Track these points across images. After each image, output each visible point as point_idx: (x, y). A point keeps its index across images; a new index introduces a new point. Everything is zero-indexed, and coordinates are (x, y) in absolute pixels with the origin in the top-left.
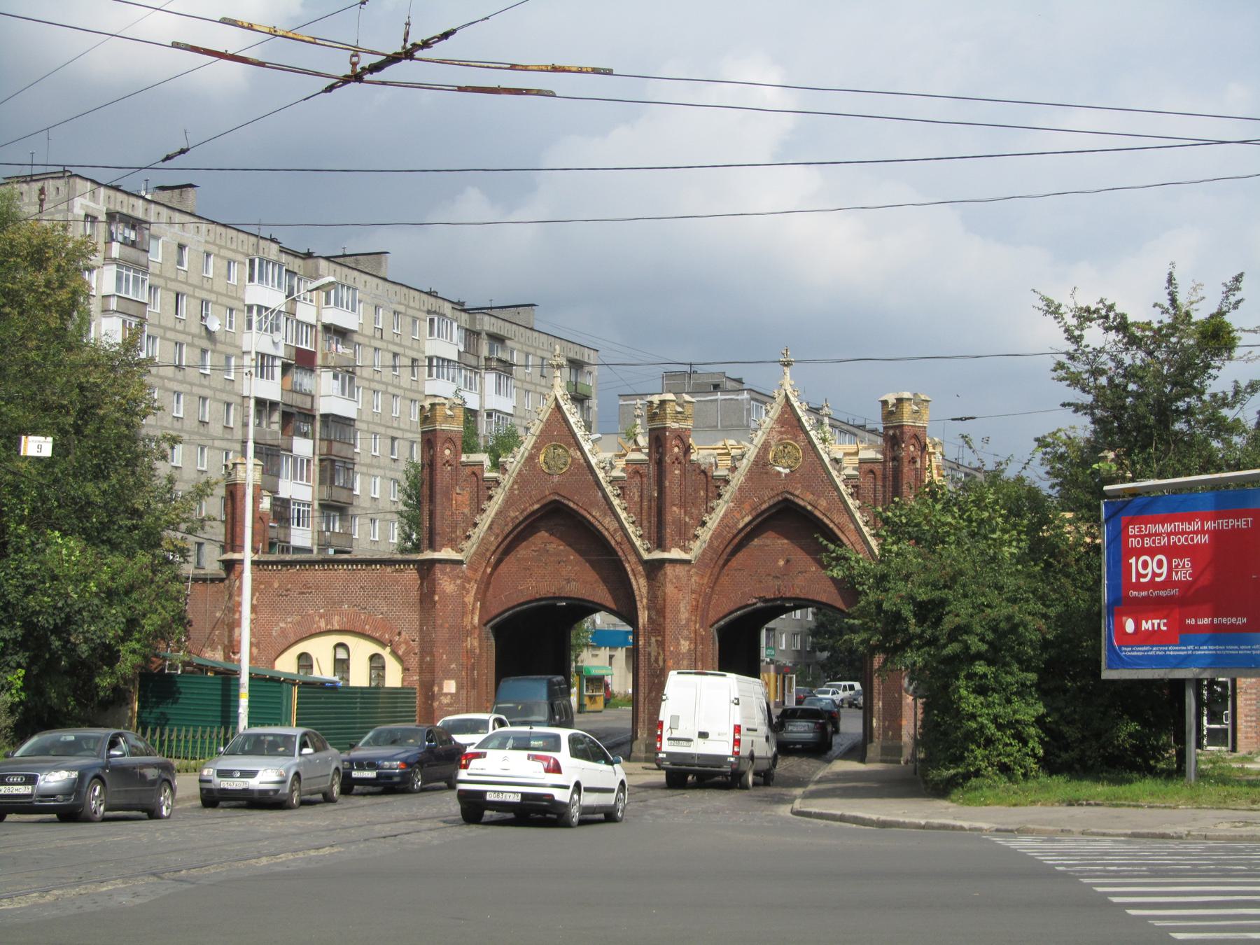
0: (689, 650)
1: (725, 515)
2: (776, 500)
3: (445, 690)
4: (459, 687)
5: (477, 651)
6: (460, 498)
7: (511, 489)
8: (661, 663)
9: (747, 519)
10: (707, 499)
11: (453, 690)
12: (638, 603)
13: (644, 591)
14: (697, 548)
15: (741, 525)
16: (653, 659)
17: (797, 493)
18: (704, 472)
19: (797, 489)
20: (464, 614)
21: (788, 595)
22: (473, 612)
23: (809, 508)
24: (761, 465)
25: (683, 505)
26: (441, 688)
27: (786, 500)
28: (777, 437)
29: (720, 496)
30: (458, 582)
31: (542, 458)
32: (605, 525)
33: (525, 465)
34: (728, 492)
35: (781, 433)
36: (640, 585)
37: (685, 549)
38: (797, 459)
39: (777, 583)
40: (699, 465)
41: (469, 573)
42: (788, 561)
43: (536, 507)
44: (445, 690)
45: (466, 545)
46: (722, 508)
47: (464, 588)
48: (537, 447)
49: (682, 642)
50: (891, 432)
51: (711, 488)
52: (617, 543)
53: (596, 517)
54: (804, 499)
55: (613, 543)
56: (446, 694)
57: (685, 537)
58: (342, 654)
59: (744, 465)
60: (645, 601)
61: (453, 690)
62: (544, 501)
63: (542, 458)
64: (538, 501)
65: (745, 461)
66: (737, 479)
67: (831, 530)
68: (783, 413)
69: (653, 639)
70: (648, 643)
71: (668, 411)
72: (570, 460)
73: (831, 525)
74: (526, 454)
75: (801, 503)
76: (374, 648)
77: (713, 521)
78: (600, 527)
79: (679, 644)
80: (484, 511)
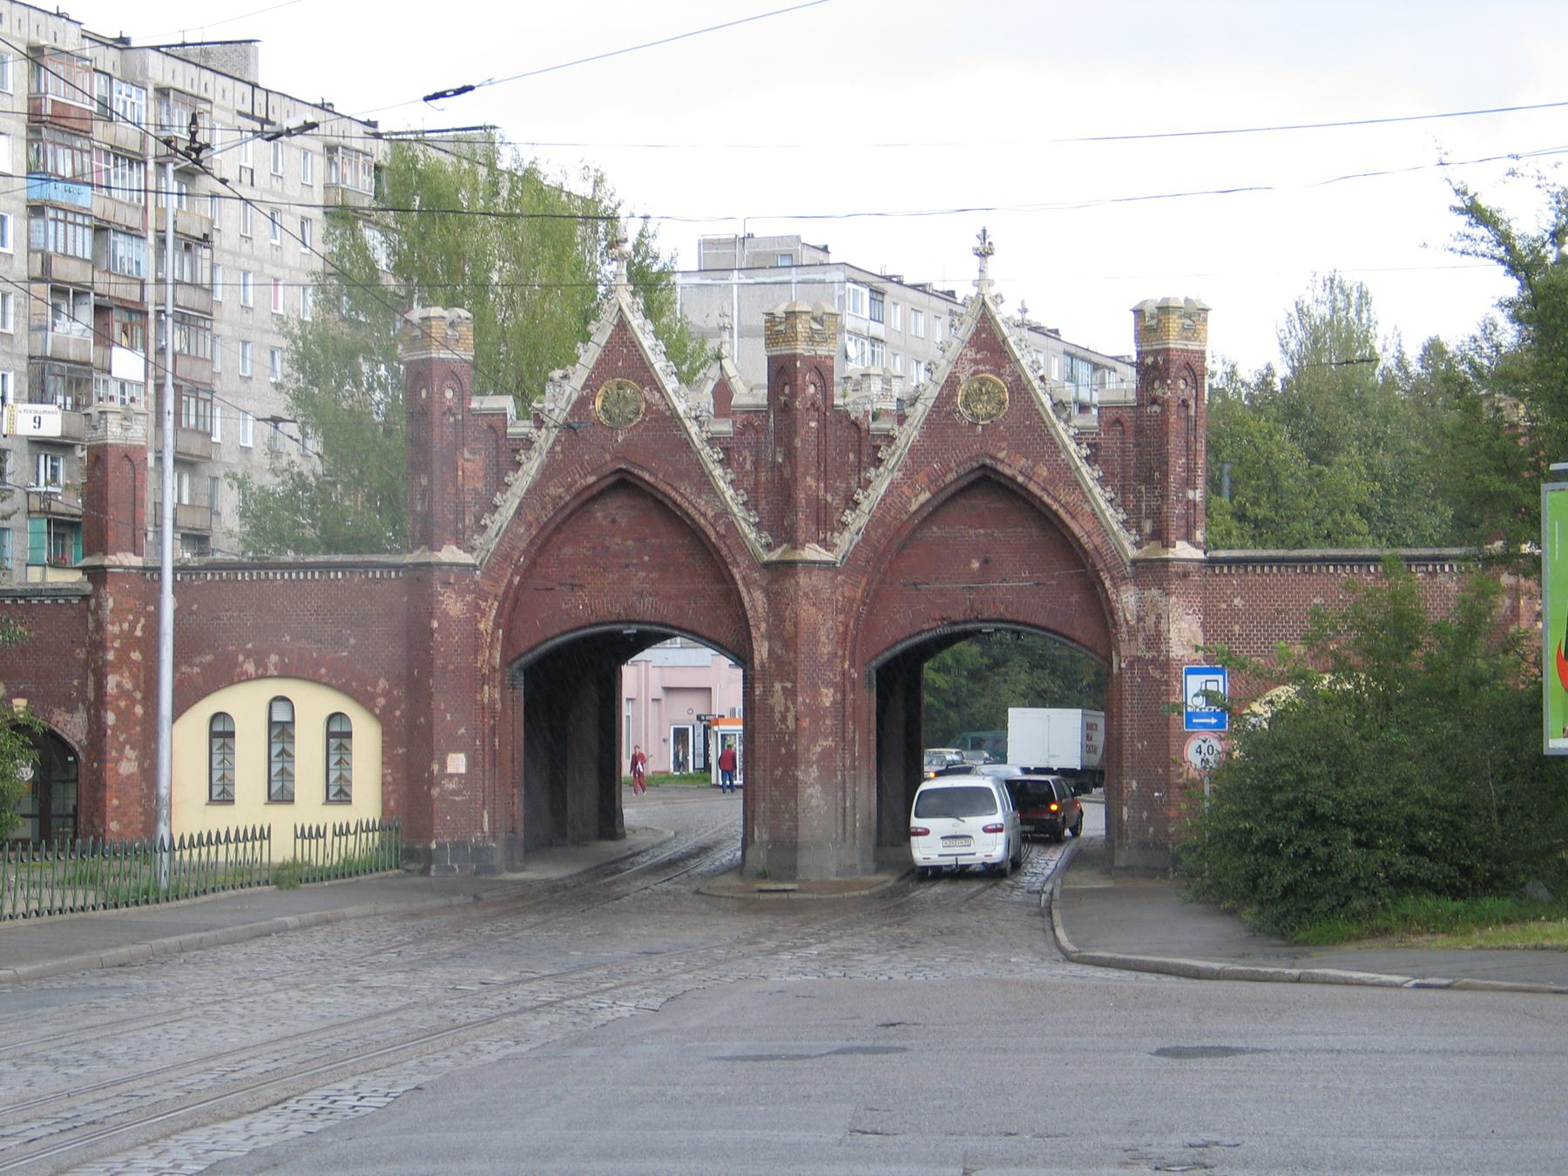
0: (834, 702)
1: (889, 492)
2: (968, 467)
3: (450, 770)
4: (471, 764)
5: (498, 706)
6: (468, 465)
7: (551, 451)
8: (791, 723)
9: (924, 497)
10: (860, 468)
11: (463, 770)
12: (753, 631)
14: (845, 542)
15: (914, 507)
16: (777, 716)
17: (1002, 455)
18: (855, 424)
19: (1001, 449)
20: (477, 649)
21: (986, 615)
22: (491, 647)
23: (1020, 479)
25: (823, 476)
26: (444, 765)
27: (984, 466)
28: (969, 369)
29: (878, 462)
30: (469, 598)
31: (599, 402)
32: (700, 508)
33: (572, 414)
34: (894, 458)
35: (976, 362)
36: (755, 601)
37: (828, 545)
40: (847, 414)
41: (487, 586)
42: (986, 561)
43: (591, 479)
44: (450, 770)
45: (478, 540)
46: (881, 482)
47: (477, 607)
48: (591, 385)
50: (1149, 360)
51: (866, 450)
52: (720, 536)
53: (684, 495)
54: (1013, 466)
55: (713, 537)
56: (452, 776)
57: (825, 523)
58: (280, 715)
59: (918, 413)
60: (763, 626)
61: (463, 770)
63: (599, 402)
64: (593, 472)
65: (919, 407)
66: (908, 435)
67: (1055, 514)
68: (978, 332)
69: (778, 686)
70: (769, 691)
71: (800, 328)
72: (643, 406)
73: (1055, 507)
74: (574, 397)
75: (1008, 471)
76: (334, 702)
77: (869, 501)
78: (691, 511)
80: (508, 485)
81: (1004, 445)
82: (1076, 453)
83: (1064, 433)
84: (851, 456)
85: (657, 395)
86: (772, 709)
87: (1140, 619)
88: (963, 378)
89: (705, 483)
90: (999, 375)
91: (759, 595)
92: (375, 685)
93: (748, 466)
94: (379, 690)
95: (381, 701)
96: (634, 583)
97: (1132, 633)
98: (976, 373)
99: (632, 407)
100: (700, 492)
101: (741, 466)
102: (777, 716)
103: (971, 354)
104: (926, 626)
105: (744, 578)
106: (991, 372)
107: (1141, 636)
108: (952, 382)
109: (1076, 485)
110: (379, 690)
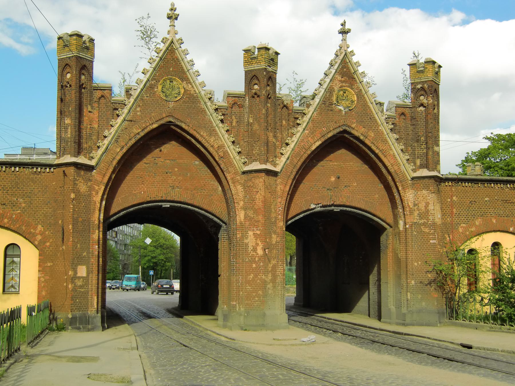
3: (79, 275)
12: (236, 205)
13: (241, 195)
19: (353, 123)
24: (327, 104)
27: (345, 131)
28: (339, 85)
31: (160, 87)
37: (275, 165)
38: (352, 102)
39: (330, 193)
43: (155, 126)
44: (79, 275)
49: (273, 236)
50: (419, 86)
53: (202, 135)
54: (358, 131)
56: (79, 278)
60: (242, 203)
61: (85, 275)
62: (162, 122)
65: (317, 100)
68: (343, 68)
69: (251, 233)
72: (182, 91)
79: (271, 237)
81: (355, 121)
82: (385, 128)
83: (380, 118)
84: (284, 122)
85: (190, 86)
86: (247, 245)
87: (415, 205)
88: (336, 89)
89: (212, 132)
90: (352, 89)
91: (240, 188)
92: (35, 228)
93: (234, 124)
94: (37, 232)
95: (39, 237)
96: (170, 181)
97: (411, 212)
98: (341, 87)
99: (177, 91)
100: (210, 135)
101: (231, 123)
102: (250, 248)
103: (339, 78)
104: (310, 208)
105: (232, 179)
106: (348, 87)
107: (416, 213)
108: (330, 91)
109: (385, 141)
110: (37, 232)
